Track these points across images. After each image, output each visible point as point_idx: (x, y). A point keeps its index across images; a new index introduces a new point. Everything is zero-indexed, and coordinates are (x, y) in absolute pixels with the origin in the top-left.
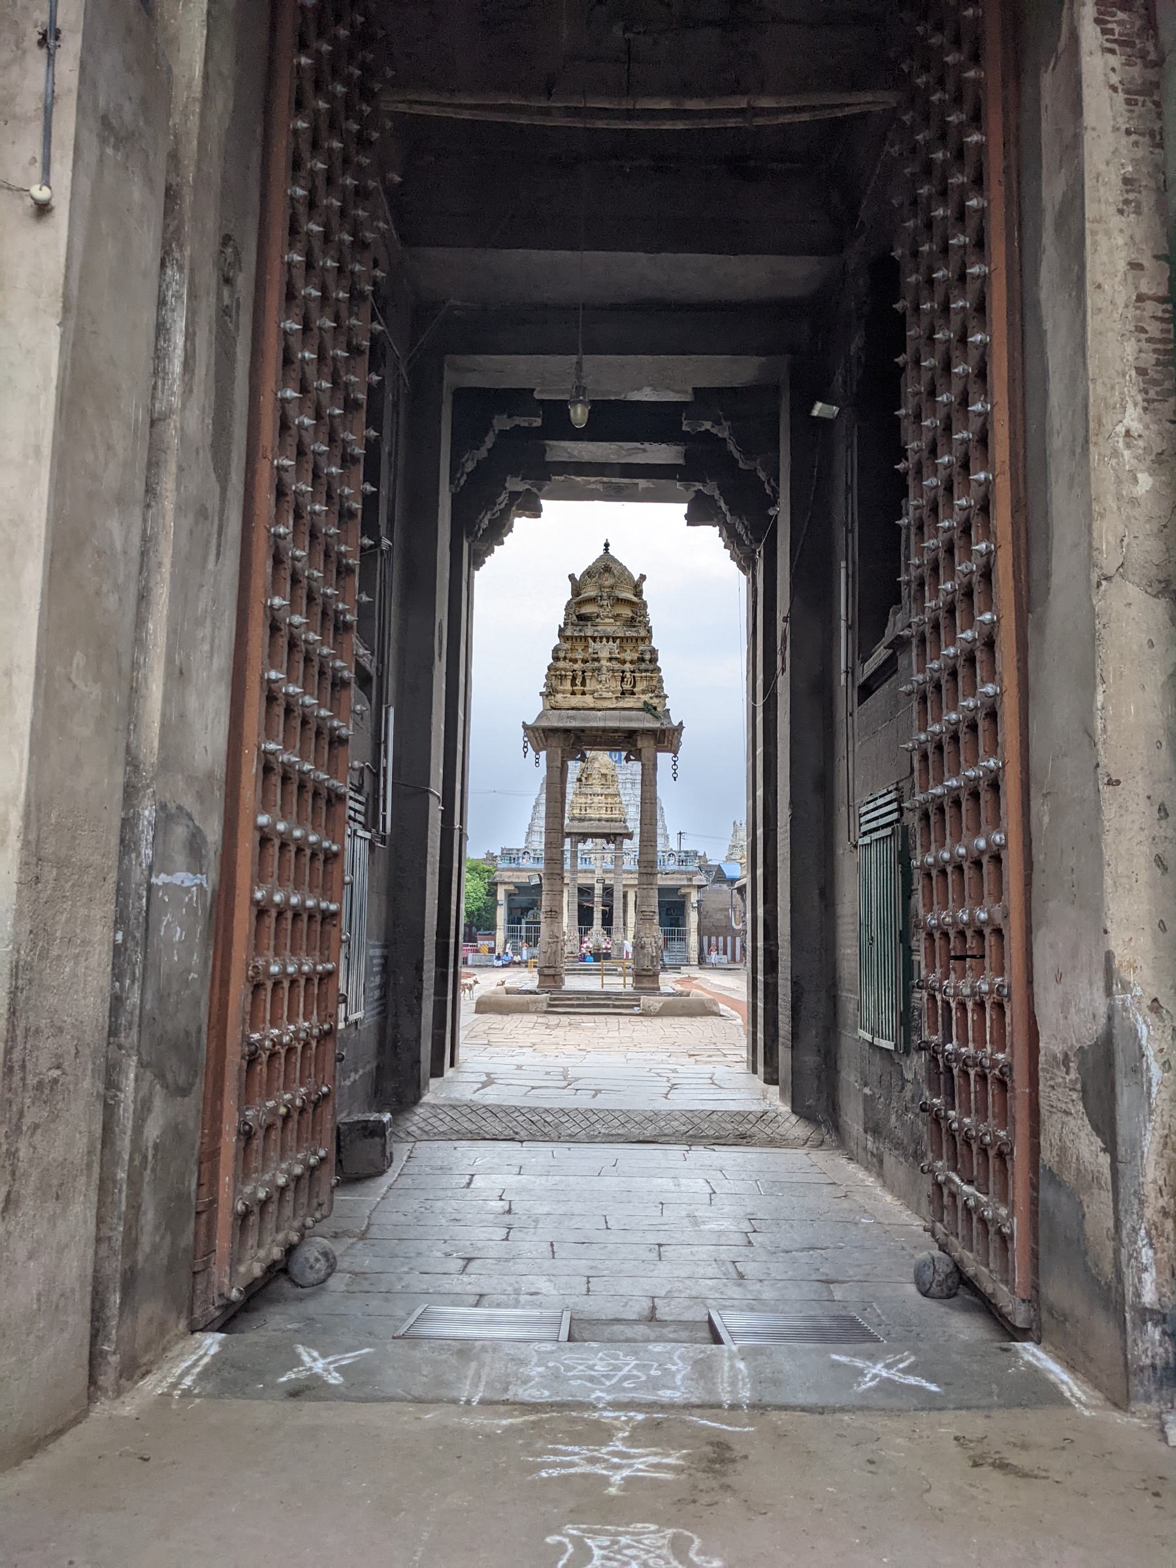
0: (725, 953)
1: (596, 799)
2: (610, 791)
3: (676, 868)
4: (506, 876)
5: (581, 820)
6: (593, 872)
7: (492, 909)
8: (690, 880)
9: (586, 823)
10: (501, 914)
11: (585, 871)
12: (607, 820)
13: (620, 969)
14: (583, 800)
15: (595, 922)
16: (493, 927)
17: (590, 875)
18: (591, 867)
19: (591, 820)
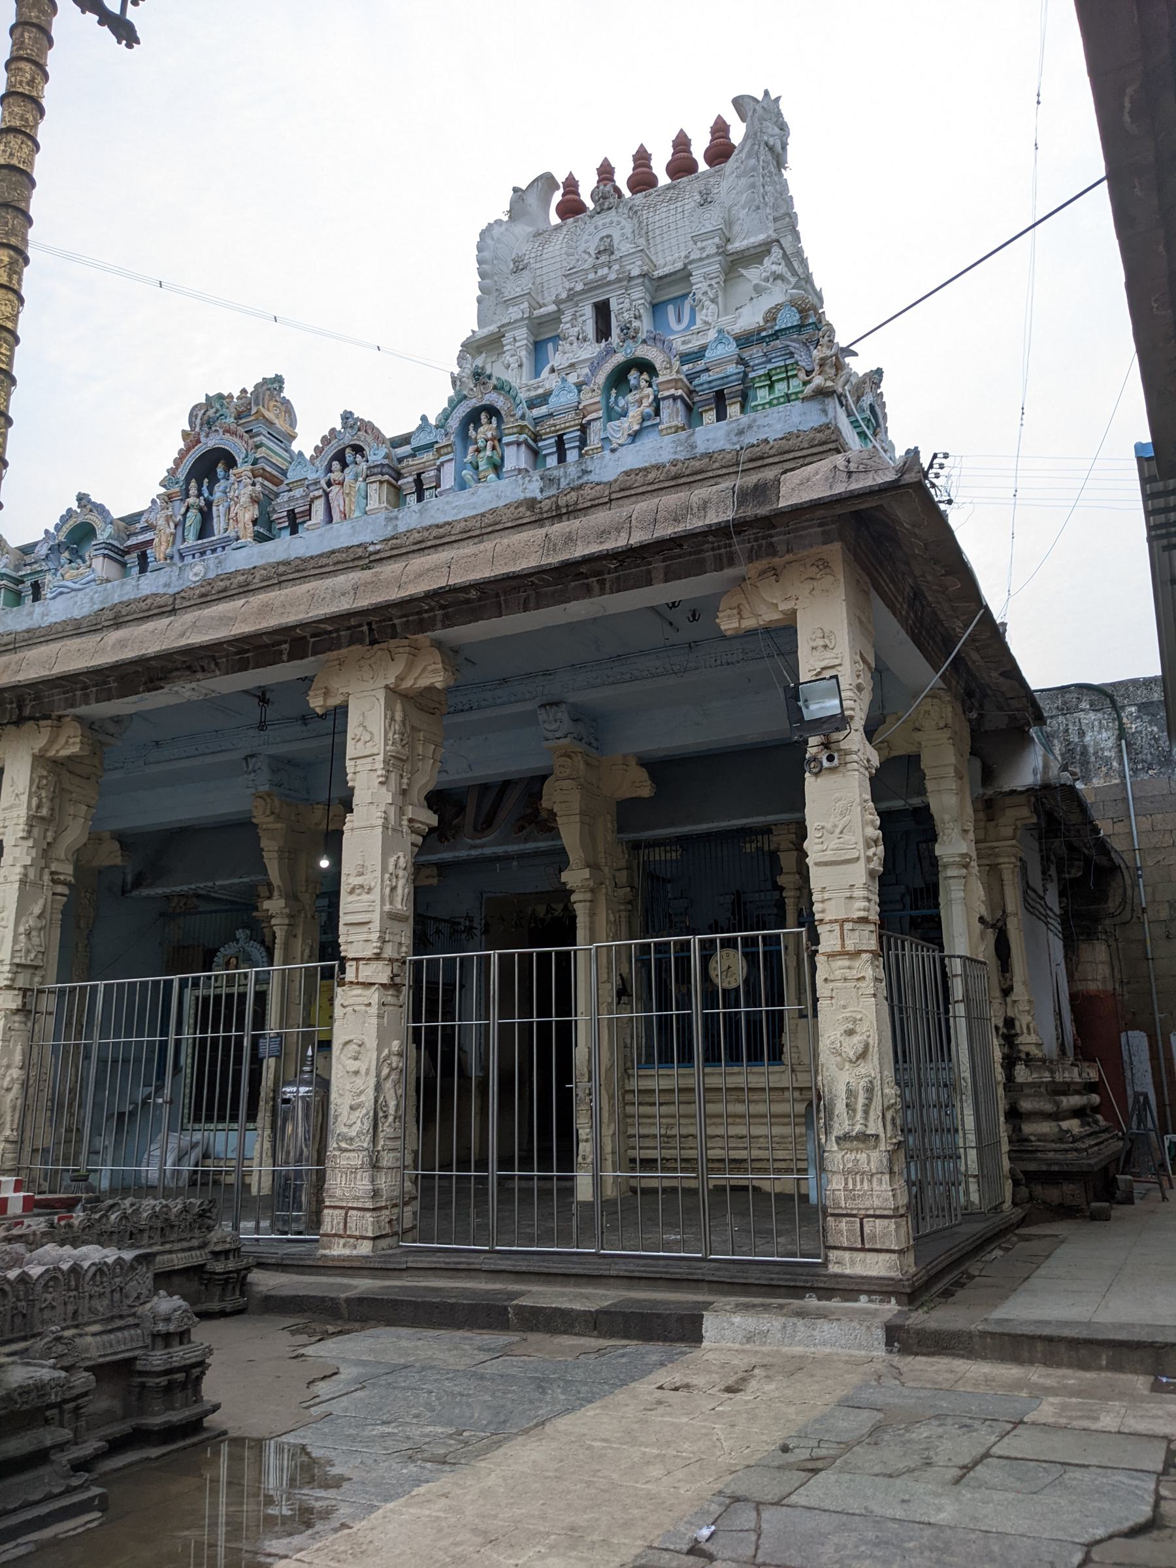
3: (658, 449)
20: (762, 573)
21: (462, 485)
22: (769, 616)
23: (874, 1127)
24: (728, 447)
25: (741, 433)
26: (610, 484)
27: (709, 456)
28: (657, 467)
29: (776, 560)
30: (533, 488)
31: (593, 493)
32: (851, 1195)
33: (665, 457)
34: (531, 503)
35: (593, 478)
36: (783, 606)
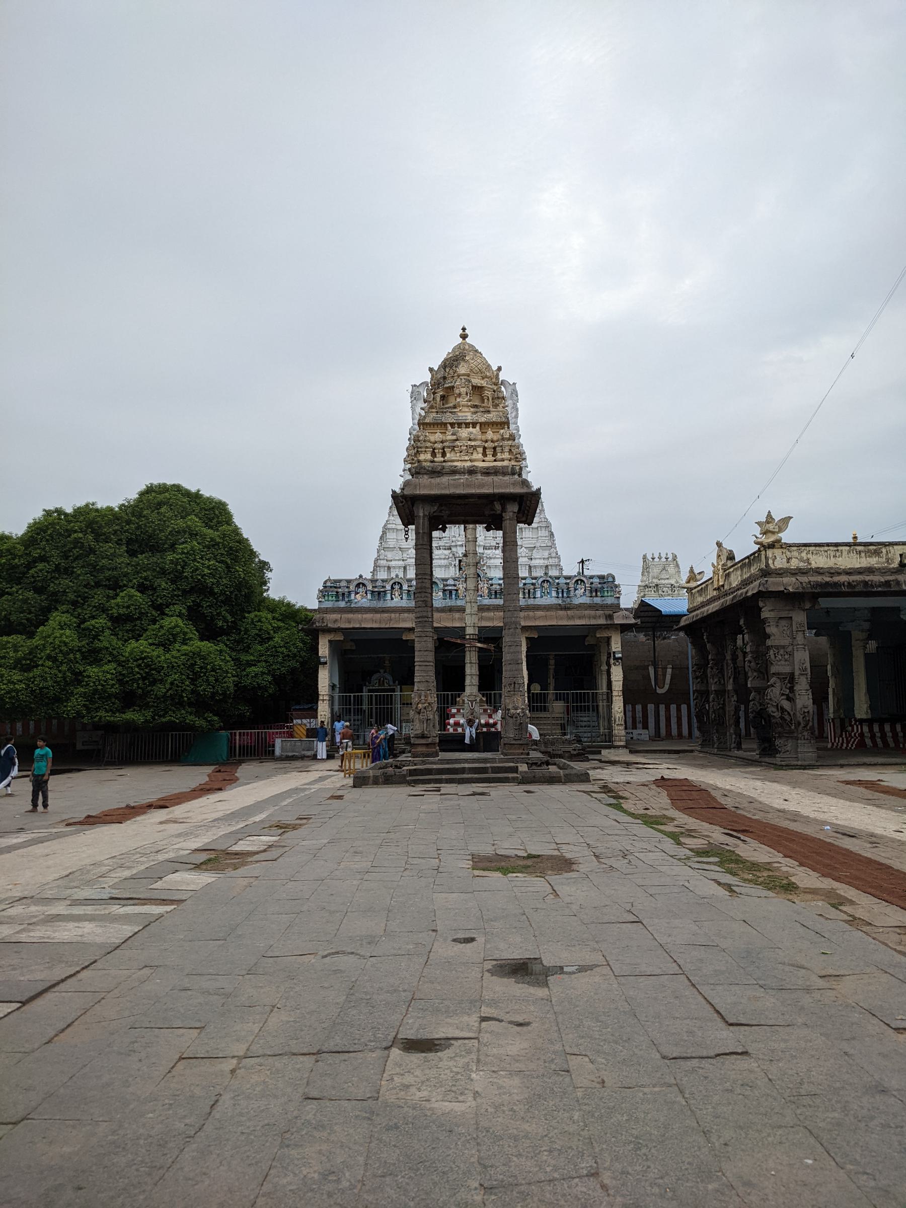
0: (645, 727)
1: (464, 433)
2: (493, 416)
3: (586, 600)
4: (331, 620)
5: (435, 473)
6: (462, 610)
7: (312, 665)
8: (610, 617)
9: (445, 479)
10: (324, 679)
11: (451, 609)
12: (487, 472)
13: (523, 768)
14: (438, 436)
15: (467, 682)
16: (314, 697)
17: (457, 615)
18: (459, 603)
19: (454, 472)
21: (542, 597)
30: (560, 602)
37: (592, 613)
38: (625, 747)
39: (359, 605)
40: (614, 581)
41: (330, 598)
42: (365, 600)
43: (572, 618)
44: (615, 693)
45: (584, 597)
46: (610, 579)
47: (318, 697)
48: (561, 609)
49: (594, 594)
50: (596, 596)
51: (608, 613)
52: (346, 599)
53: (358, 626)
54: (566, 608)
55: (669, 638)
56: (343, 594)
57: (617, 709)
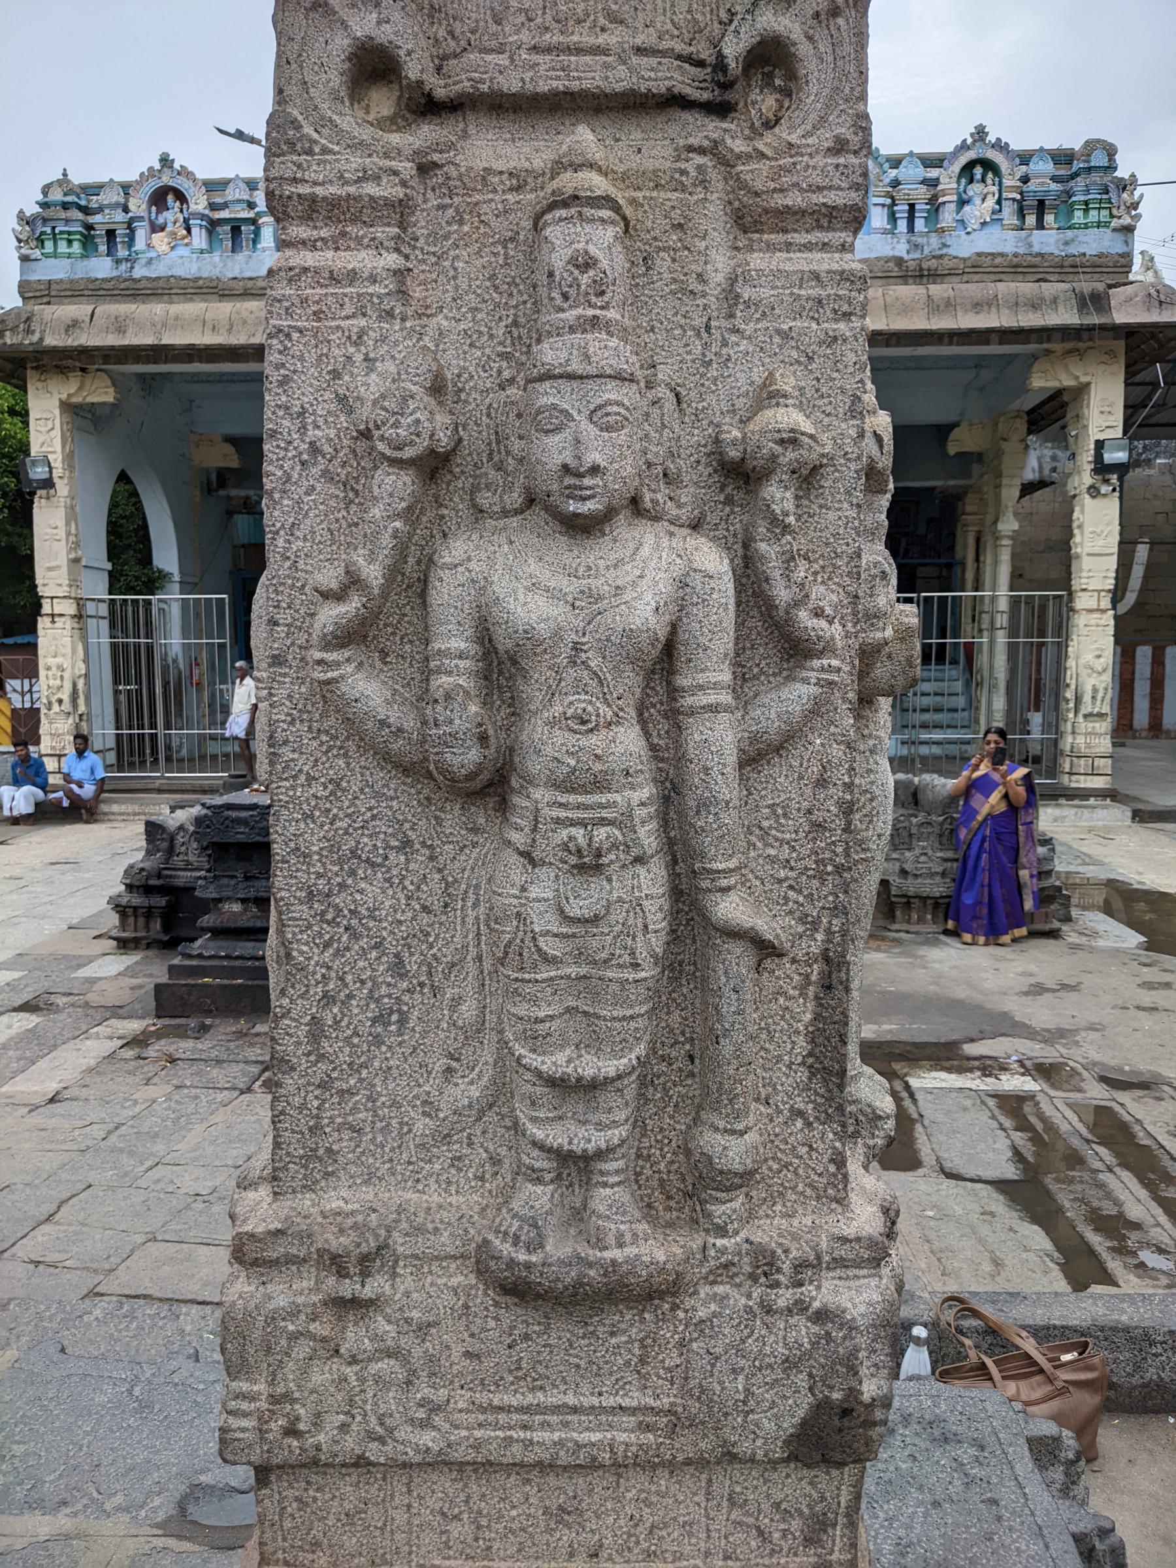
3: (1003, 241)
8: (1098, 301)
20: (1070, 352)
22: (1068, 382)
23: (1106, 709)
24: (1057, 252)
25: (1066, 243)
26: (965, 260)
27: (1041, 255)
28: (1002, 255)
29: (1081, 345)
30: (901, 249)
31: (951, 264)
32: (1088, 746)
33: (1009, 248)
34: (899, 261)
35: (951, 251)
36: (1083, 379)
37: (1027, 288)
38: (1112, 795)
39: (159, 270)
40: (1111, 167)
41: (63, 247)
42: (182, 251)
43: (949, 305)
44: (1083, 602)
45: (995, 230)
46: (1098, 159)
47: (40, 606)
48: (904, 278)
49: (1031, 220)
50: (1040, 226)
51: (1086, 286)
52: (122, 252)
53: (149, 340)
54: (923, 275)
55: (1149, 462)
56: (111, 234)
57: (1088, 657)
